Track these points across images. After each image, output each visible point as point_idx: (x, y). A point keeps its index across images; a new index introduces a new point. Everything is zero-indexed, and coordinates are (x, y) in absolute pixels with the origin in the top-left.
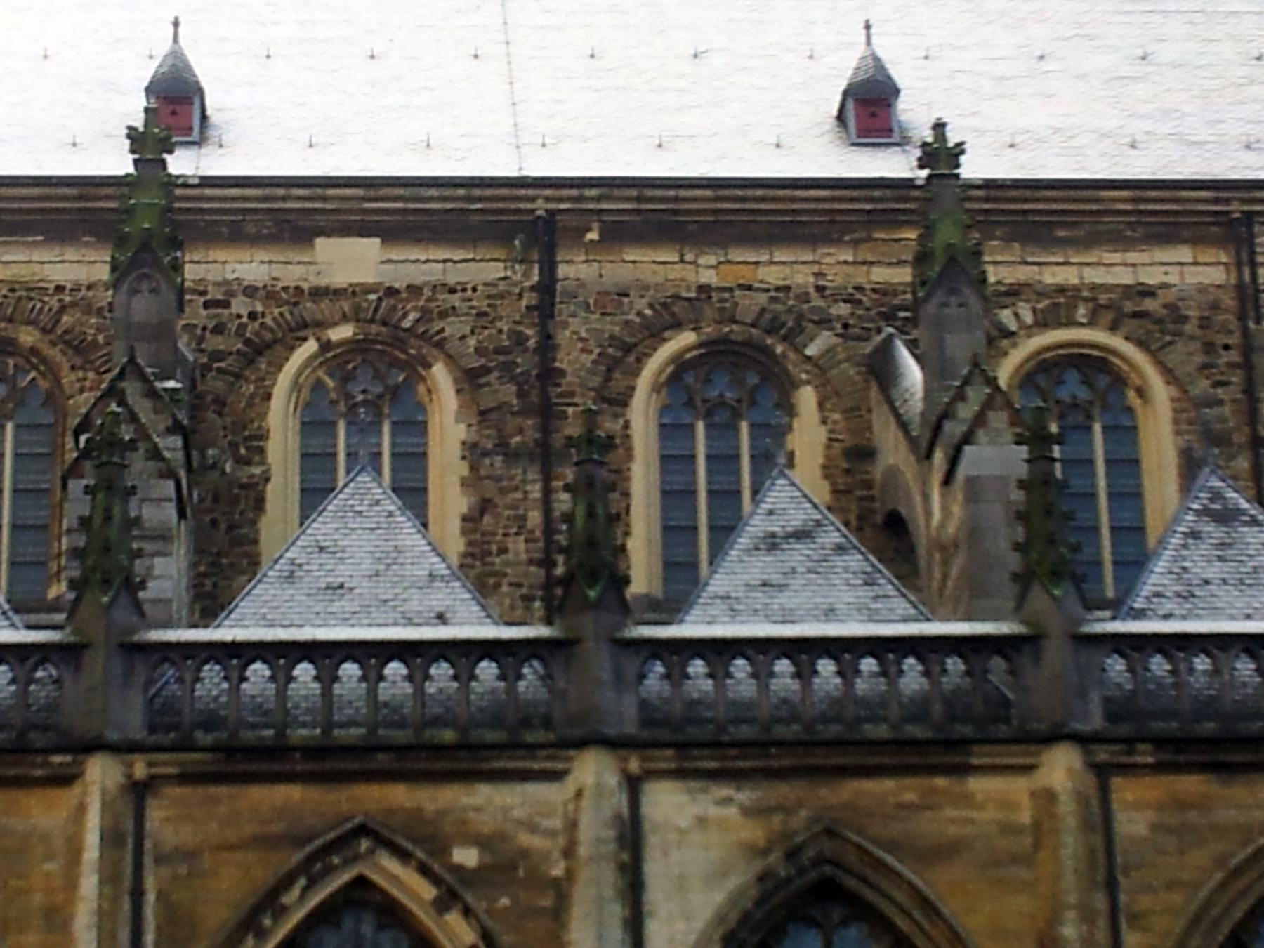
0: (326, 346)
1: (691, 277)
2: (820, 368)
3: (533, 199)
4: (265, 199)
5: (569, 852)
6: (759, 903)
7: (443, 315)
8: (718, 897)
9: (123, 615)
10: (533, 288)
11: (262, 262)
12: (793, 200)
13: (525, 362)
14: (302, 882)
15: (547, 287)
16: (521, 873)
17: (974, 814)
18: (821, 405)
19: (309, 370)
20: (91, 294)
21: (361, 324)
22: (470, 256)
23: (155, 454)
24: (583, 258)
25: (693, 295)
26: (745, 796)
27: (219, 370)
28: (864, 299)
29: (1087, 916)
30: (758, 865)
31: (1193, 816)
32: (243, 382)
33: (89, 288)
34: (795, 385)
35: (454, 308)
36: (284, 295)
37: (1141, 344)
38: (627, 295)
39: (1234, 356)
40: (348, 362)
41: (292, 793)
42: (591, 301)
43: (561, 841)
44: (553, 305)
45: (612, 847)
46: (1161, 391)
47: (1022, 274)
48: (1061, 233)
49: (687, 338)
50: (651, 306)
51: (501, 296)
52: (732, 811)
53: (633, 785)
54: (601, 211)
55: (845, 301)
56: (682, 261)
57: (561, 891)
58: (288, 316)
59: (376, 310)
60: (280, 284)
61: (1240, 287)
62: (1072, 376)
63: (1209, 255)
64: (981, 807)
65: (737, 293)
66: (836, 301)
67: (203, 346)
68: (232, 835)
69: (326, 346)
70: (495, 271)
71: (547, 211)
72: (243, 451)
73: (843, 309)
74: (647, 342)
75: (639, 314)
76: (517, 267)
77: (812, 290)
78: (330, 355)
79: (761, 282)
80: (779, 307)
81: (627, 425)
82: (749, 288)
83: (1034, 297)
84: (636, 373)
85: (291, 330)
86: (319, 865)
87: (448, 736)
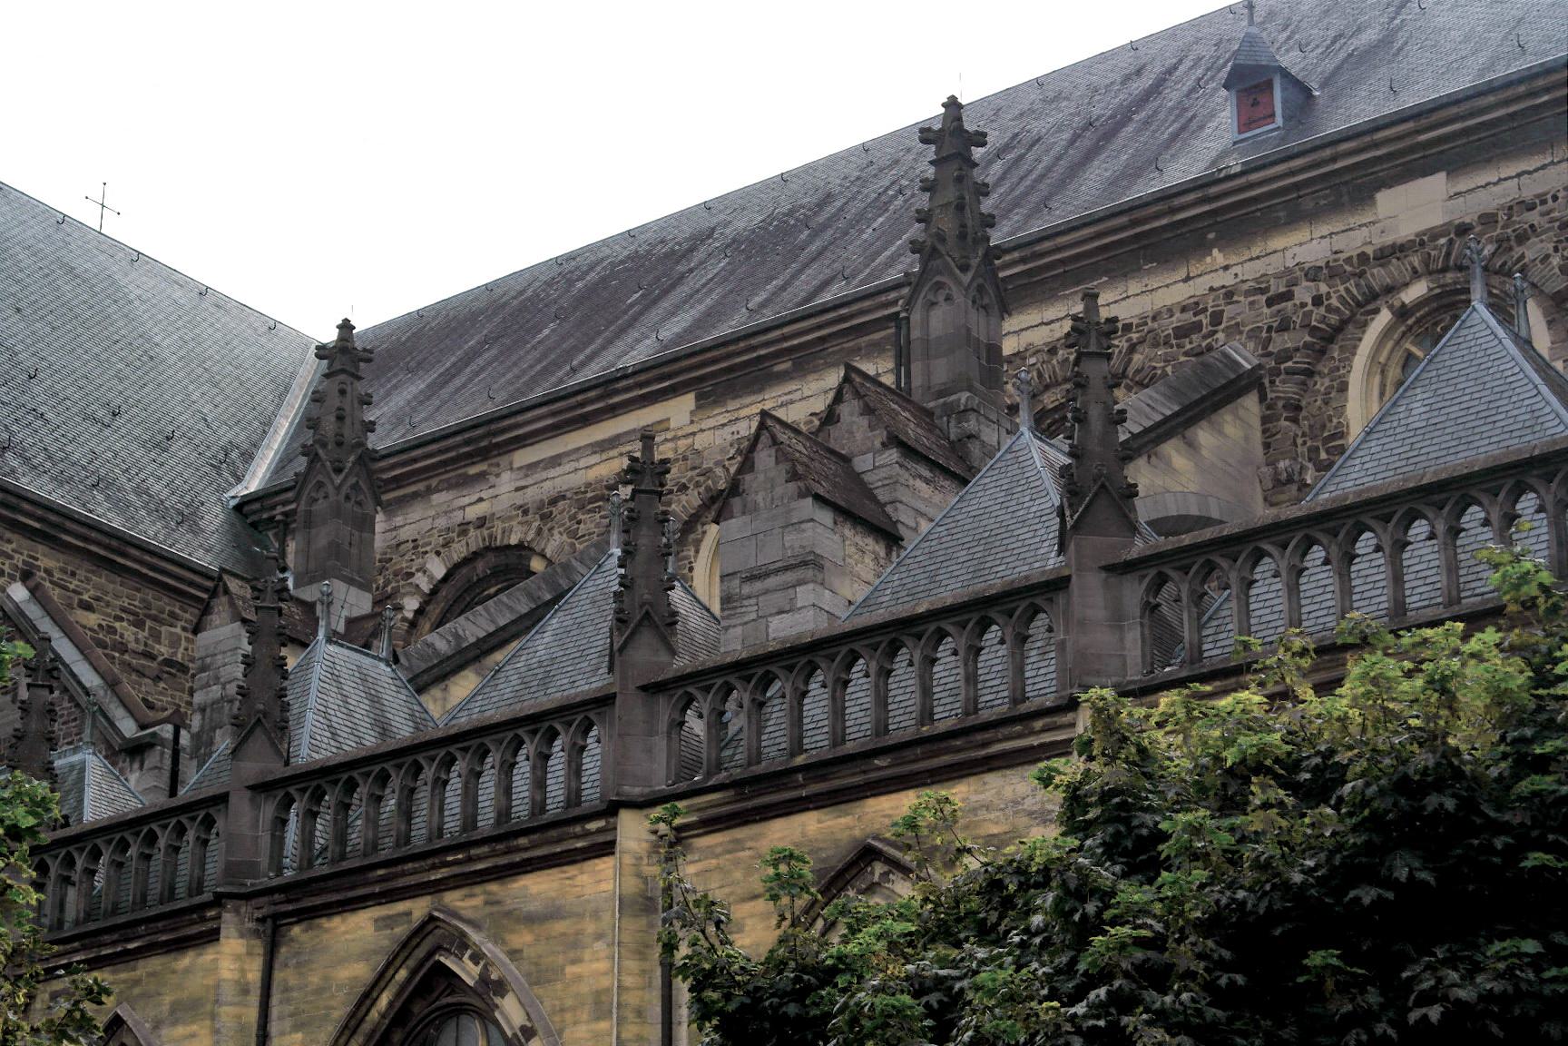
0: (1402, 313)
7: (1522, 238)
11: (1322, 237)
19: (1390, 345)
20: (1156, 325)
21: (1435, 276)
27: (1289, 372)
32: (1317, 378)
33: (1154, 319)
35: (1532, 226)
36: (1348, 268)
40: (1436, 324)
58: (1355, 291)
59: (1448, 254)
60: (1343, 256)
67: (1270, 349)
69: (1402, 313)
72: (1323, 455)
78: (1410, 322)
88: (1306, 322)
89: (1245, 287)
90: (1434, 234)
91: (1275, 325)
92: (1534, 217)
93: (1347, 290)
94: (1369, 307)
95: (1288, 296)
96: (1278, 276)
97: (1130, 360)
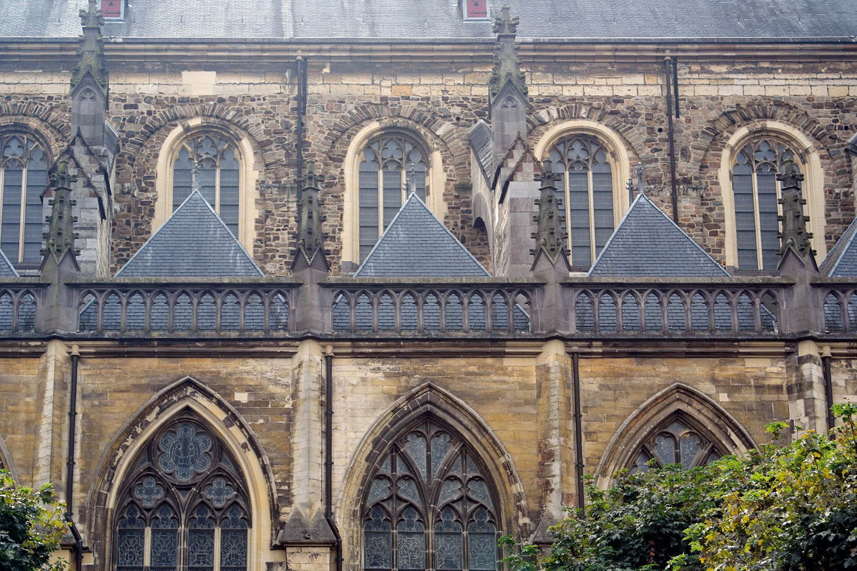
0: (187, 129)
1: (378, 92)
2: (444, 142)
3: (295, 51)
4: (157, 50)
5: (294, 396)
6: (393, 424)
7: (247, 113)
8: (372, 421)
9: (67, 268)
10: (295, 99)
12: (432, 51)
13: (290, 138)
14: (157, 409)
15: (302, 99)
16: (270, 406)
17: (507, 378)
18: (444, 161)
19: (179, 141)
21: (205, 118)
22: (263, 81)
23: (89, 184)
24: (321, 82)
25: (378, 102)
26: (388, 367)
28: (469, 104)
29: (564, 434)
30: (393, 404)
31: (621, 380)
34: (431, 151)
35: (253, 109)
37: (615, 129)
38: (344, 102)
39: (664, 135)
40: (198, 138)
41: (153, 363)
42: (325, 105)
43: (291, 390)
44: (305, 108)
45: (317, 393)
46: (624, 155)
47: (552, 91)
48: (574, 68)
49: (374, 125)
50: (356, 108)
51: (278, 103)
52: (381, 374)
53: (329, 360)
54: (330, 57)
55: (458, 105)
56: (373, 84)
57: (290, 415)
58: (168, 114)
59: (213, 110)
60: (164, 96)
61: (668, 97)
62: (577, 146)
63: (652, 80)
64: (510, 375)
65: (401, 101)
66: (453, 105)
67: (124, 129)
68: (122, 384)
69: (187, 129)
70: (274, 89)
71: (302, 57)
73: (456, 110)
74: (354, 127)
75: (350, 112)
76: (287, 87)
77: (441, 99)
78: (188, 134)
79: (414, 95)
80: (424, 109)
81: (342, 172)
82: (408, 98)
83: (558, 103)
84: (348, 144)
85: (169, 121)
86: (166, 401)
87: (234, 335)
88: (143, 121)
89: (115, 96)
90: (208, 99)
91: (127, 118)
92: (254, 105)
93: (164, 112)
94: (173, 123)
95: (135, 107)
96: (131, 96)
97: (50, 114)
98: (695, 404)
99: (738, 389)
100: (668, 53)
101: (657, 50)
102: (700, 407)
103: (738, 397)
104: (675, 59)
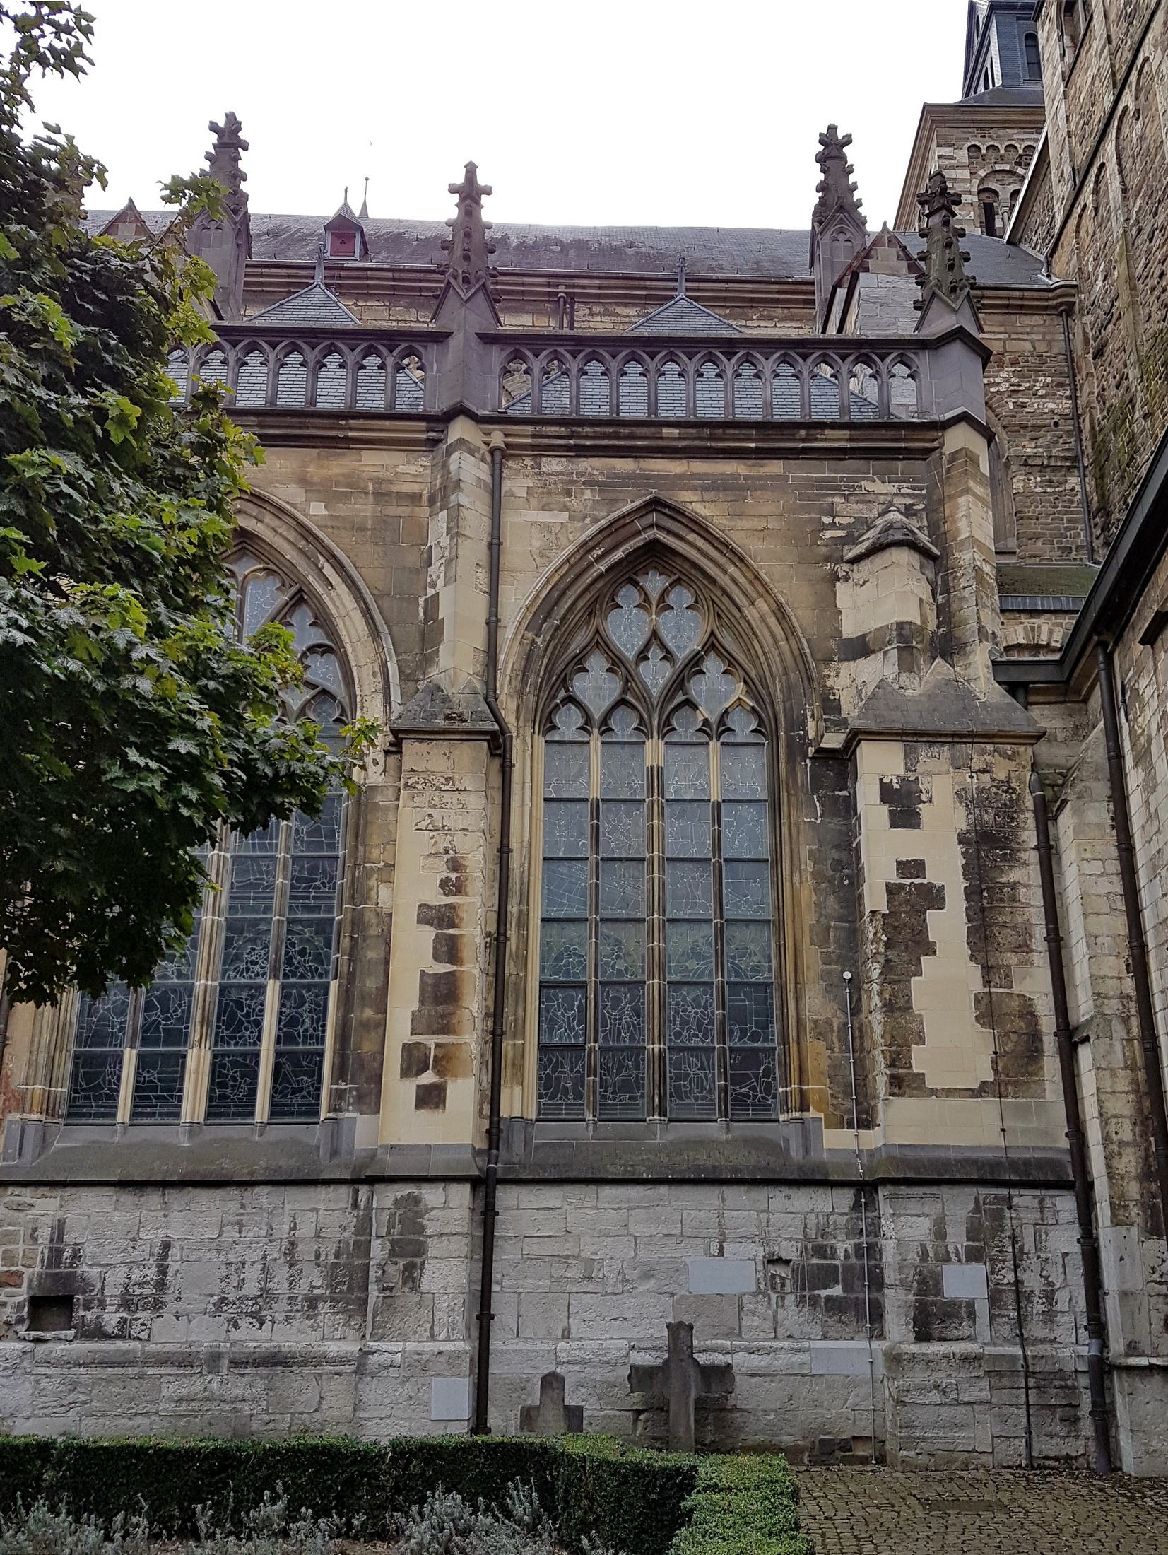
98: (268, 518)
99: (345, 497)
100: (562, 289)
101: (549, 285)
102: (276, 523)
103: (342, 509)
104: (572, 296)
